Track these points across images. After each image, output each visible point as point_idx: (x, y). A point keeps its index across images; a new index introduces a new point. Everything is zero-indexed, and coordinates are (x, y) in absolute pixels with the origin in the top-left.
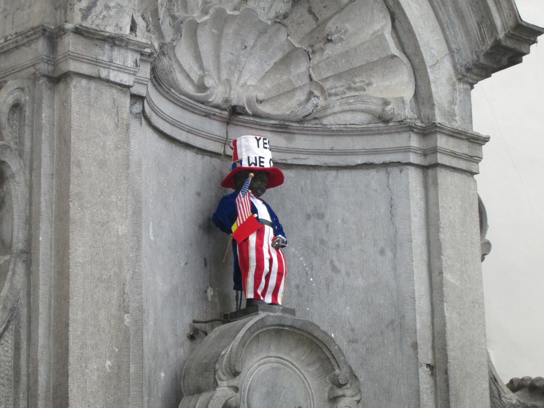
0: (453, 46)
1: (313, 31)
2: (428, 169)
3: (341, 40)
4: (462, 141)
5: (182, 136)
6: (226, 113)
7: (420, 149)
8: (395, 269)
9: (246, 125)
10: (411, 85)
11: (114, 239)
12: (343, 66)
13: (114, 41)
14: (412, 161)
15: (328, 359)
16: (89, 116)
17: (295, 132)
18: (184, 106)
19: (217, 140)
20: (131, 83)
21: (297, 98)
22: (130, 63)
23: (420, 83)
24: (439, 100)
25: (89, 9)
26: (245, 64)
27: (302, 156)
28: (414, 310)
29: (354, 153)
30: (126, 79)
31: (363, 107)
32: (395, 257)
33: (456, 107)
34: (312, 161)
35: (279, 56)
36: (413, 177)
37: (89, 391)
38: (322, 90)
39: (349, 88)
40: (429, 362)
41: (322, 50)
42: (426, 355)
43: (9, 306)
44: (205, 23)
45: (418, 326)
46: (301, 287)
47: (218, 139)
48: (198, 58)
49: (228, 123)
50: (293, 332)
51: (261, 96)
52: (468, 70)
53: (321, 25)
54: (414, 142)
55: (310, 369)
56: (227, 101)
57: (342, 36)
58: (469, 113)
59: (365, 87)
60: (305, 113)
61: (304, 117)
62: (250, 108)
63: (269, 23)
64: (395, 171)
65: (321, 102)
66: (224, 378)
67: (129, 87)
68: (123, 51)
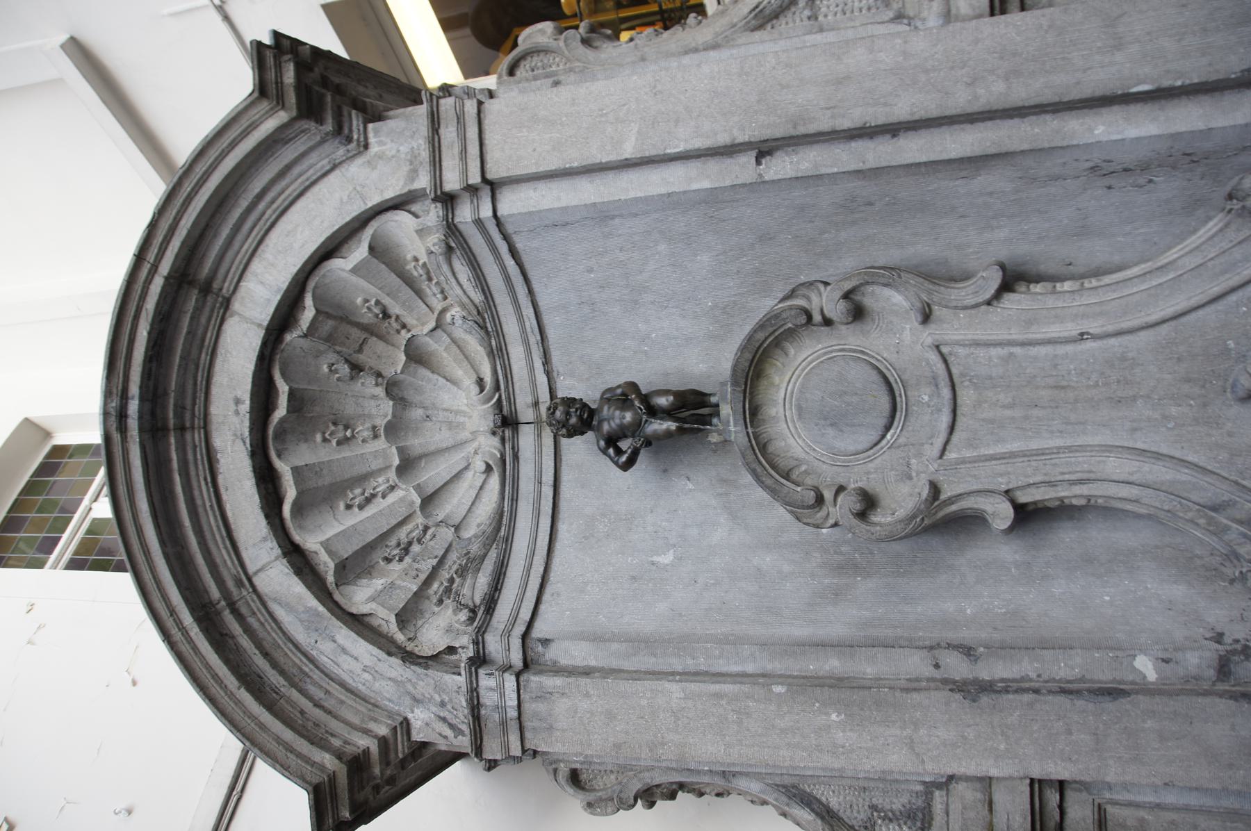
0: (328, 168)
1: (381, 337)
2: (494, 186)
3: (378, 303)
4: (442, 141)
5: (548, 491)
6: (508, 433)
7: (472, 202)
8: (636, 215)
10: (397, 218)
11: (690, 703)
12: (407, 292)
13: (475, 707)
14: (490, 213)
16: (564, 731)
18: (515, 500)
19: (540, 436)
20: (513, 678)
22: (492, 682)
23: (390, 204)
24: (401, 183)
25: (451, 726)
26: (446, 410)
27: (528, 324)
28: (685, 192)
29: (504, 269)
30: (510, 681)
31: (445, 268)
32: (621, 216)
33: (401, 148)
34: (528, 312)
35: (423, 372)
36: (512, 203)
37: (870, 744)
38: (444, 311)
39: (430, 279)
40: (754, 160)
41: (398, 317)
42: (742, 169)
43: (785, 799)
44: (418, 488)
45: (706, 184)
48: (457, 476)
51: (475, 389)
52: (349, 140)
53: (369, 330)
54: (464, 214)
55: (792, 352)
56: (494, 433)
57: (373, 302)
58: (402, 783)
59: (421, 263)
61: (482, 328)
62: (491, 398)
63: (391, 403)
64: (510, 229)
65: (456, 311)
66: (825, 508)
67: (518, 676)
68: (482, 692)
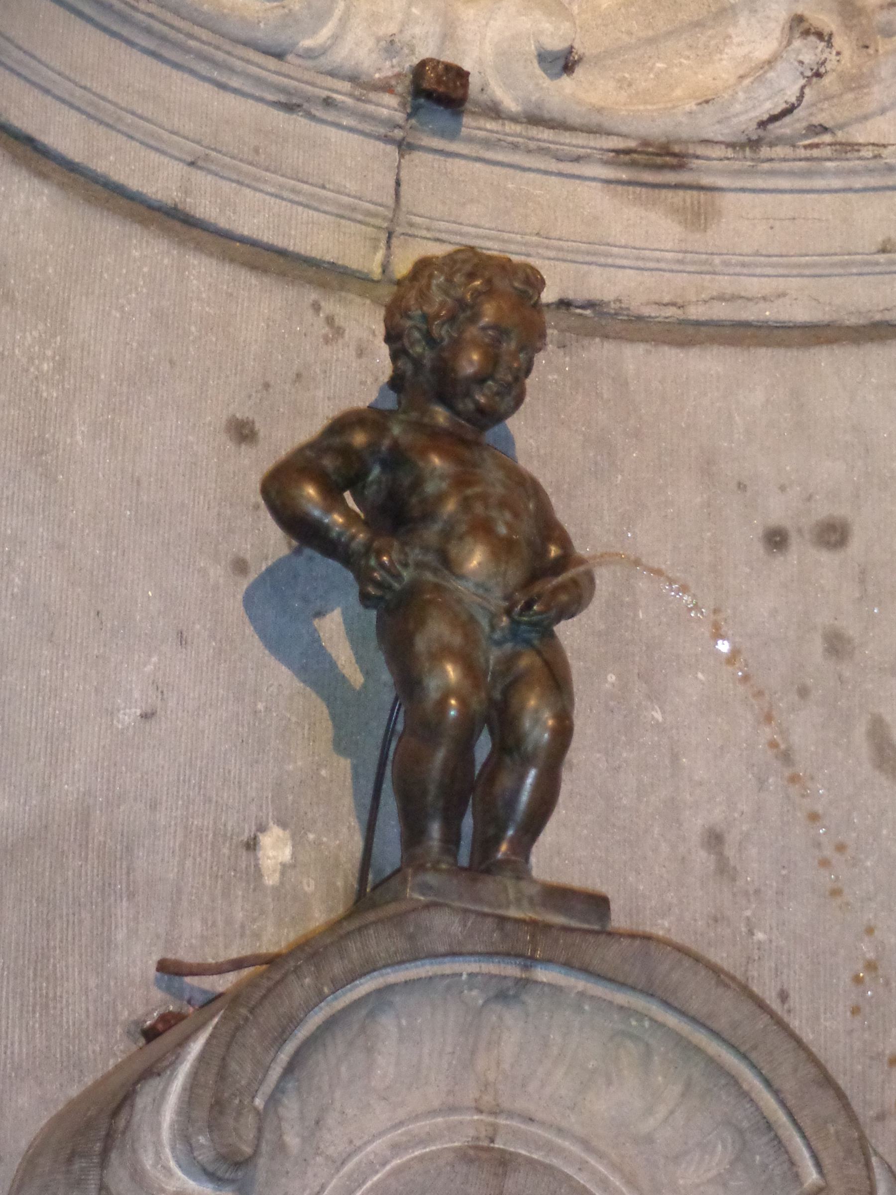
9: (490, 155)
15: (769, 1126)
17: (721, 182)
21: (741, 52)
46: (732, 838)
47: (354, 209)
49: (404, 147)
50: (582, 994)
60: (768, 105)
61: (762, 124)
